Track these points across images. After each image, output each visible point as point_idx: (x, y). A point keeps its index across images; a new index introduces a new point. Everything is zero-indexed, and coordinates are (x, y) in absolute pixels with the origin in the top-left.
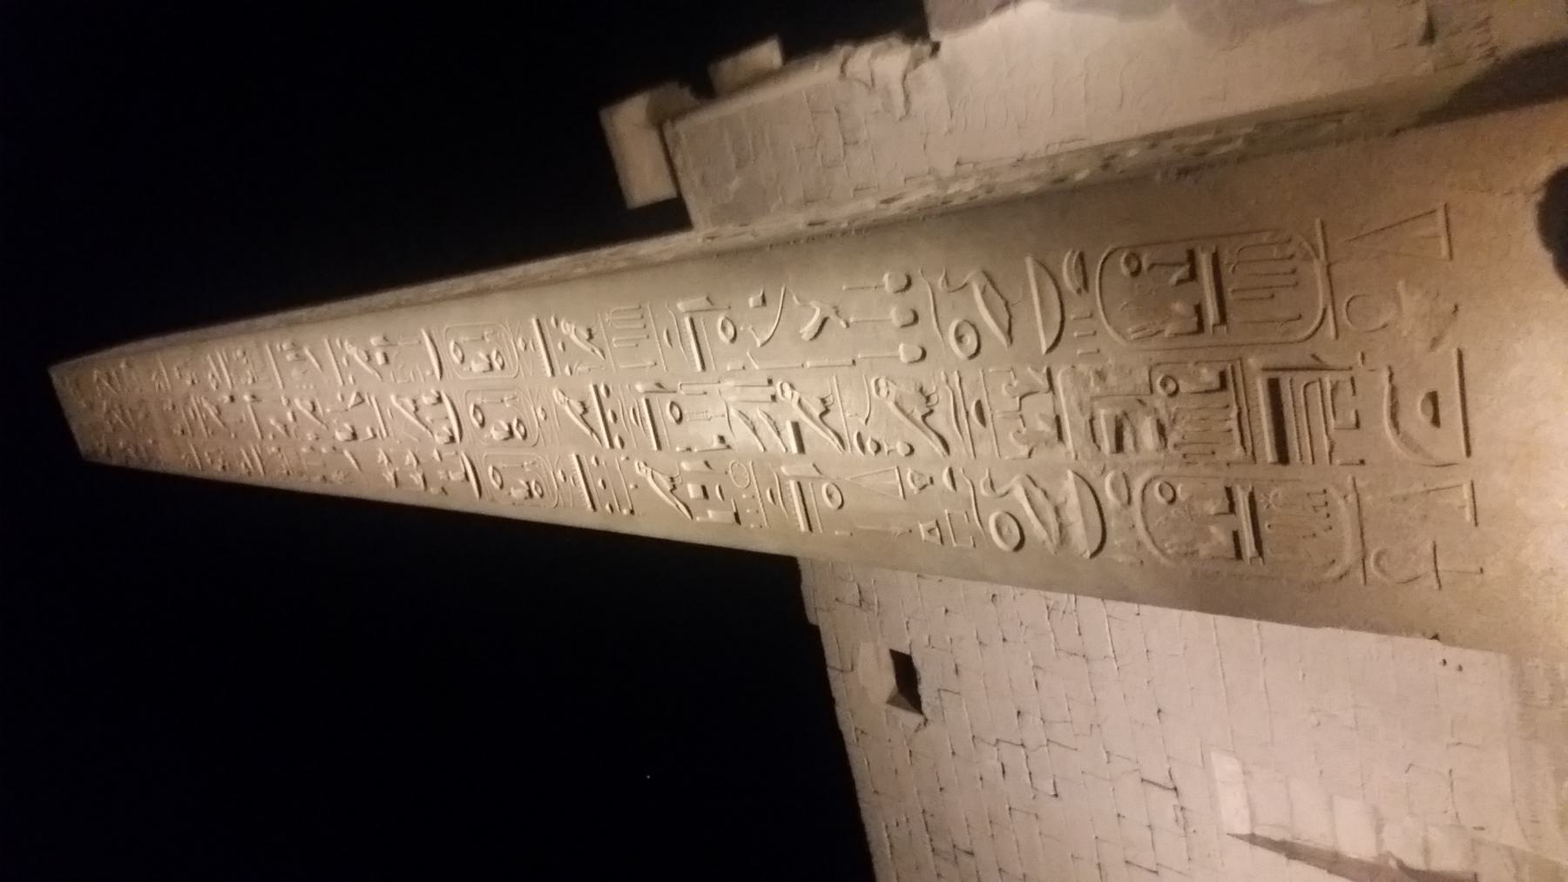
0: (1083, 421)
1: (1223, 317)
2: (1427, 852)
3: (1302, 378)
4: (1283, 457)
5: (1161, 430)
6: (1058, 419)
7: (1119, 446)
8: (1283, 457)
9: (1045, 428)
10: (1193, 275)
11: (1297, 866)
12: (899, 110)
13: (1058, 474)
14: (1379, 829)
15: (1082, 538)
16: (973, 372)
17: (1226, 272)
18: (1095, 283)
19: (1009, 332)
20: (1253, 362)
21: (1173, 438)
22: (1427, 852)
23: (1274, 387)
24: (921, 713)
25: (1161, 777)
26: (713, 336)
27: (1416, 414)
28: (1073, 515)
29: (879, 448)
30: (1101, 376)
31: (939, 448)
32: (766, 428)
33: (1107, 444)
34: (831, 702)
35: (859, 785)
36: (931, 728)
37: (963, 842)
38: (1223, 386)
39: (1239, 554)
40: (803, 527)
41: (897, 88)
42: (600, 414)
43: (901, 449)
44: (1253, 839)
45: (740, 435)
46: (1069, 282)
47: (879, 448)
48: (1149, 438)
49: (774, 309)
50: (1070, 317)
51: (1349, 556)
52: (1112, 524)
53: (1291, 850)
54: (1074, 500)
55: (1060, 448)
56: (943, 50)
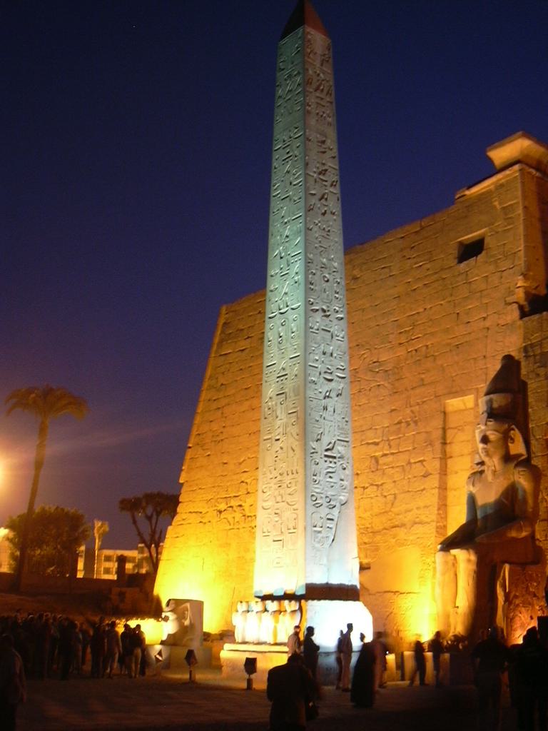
9: (278, 500)
27: (277, 560)
29: (276, 461)
40: (265, 438)
45: (278, 423)
49: (297, 437)
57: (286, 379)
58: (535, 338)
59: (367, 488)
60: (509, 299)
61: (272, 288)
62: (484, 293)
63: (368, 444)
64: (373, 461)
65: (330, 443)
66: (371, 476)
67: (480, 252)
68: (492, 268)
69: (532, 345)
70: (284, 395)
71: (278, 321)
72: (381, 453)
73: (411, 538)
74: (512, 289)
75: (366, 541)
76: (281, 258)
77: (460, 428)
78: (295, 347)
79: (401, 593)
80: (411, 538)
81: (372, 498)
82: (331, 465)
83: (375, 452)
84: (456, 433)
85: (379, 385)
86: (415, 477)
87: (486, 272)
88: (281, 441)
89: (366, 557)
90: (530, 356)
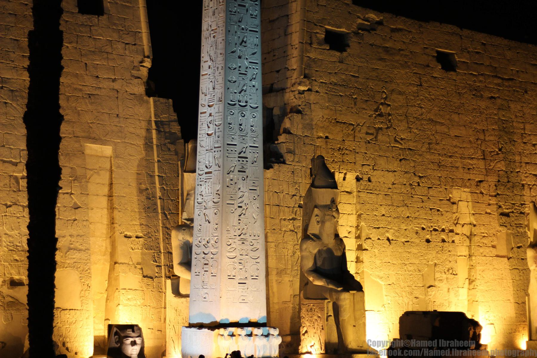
40: (228, 202)
49: (257, 209)
51: (229, 289)
58: (164, 117)
59: (10, 206)
60: (135, 72)
62: (110, 56)
63: (4, 162)
64: (13, 181)
66: (14, 195)
68: (115, 36)
69: (162, 122)
72: (21, 175)
73: (68, 261)
74: (136, 64)
75: (17, 258)
77: (96, 171)
79: (63, 310)
80: (68, 261)
81: (18, 218)
83: (14, 172)
85: (6, 103)
86: (65, 207)
87: (110, 37)
89: (19, 273)
90: (162, 132)
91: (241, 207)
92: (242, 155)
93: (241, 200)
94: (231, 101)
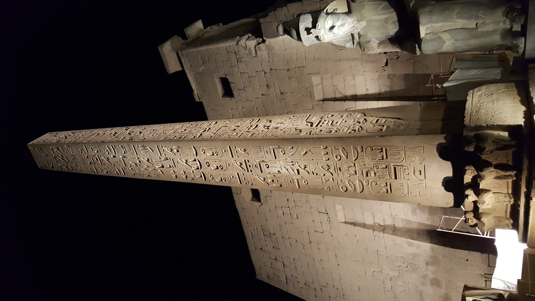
0: (360, 172)
1: (387, 158)
2: (384, 221)
3: (400, 167)
4: (396, 178)
5: (375, 174)
6: (356, 171)
7: (367, 176)
8: (396, 178)
9: (353, 172)
10: (382, 151)
11: (357, 228)
12: (254, 55)
13: (355, 180)
14: (374, 217)
15: (359, 190)
16: (339, 163)
17: (388, 152)
18: (364, 151)
19: (347, 157)
20: (392, 165)
21: (377, 175)
22: (384, 221)
23: (395, 169)
24: (260, 202)
25: (324, 211)
26: (279, 153)
28: (357, 186)
29: (317, 174)
30: (364, 165)
31: (331, 175)
32: (290, 170)
33: (365, 175)
34: (234, 202)
35: (242, 221)
36: (263, 205)
37: (272, 232)
38: (386, 168)
39: (387, 192)
40: (298, 187)
41: (253, 49)
42: (246, 166)
43: (322, 175)
44: (346, 223)
45: (284, 171)
46: (359, 151)
47: (317, 174)
48: (373, 175)
49: (295, 149)
50: (359, 155)
52: (365, 188)
53: (354, 224)
54: (358, 184)
55: (356, 176)
56: (266, 42)
57: (248, 161)
61: (184, 177)
65: (307, 125)
67: (227, 79)
70: (261, 164)
71: (206, 170)
76: (163, 167)
78: (223, 151)
82: (326, 123)
84: (339, 91)
88: (299, 168)
91: (298, 170)
92: (244, 166)
93: (290, 170)
94: (201, 176)
